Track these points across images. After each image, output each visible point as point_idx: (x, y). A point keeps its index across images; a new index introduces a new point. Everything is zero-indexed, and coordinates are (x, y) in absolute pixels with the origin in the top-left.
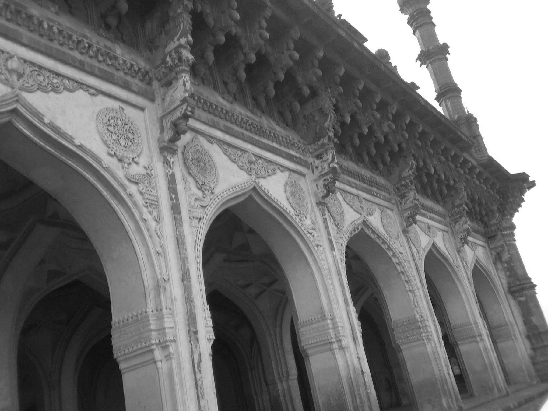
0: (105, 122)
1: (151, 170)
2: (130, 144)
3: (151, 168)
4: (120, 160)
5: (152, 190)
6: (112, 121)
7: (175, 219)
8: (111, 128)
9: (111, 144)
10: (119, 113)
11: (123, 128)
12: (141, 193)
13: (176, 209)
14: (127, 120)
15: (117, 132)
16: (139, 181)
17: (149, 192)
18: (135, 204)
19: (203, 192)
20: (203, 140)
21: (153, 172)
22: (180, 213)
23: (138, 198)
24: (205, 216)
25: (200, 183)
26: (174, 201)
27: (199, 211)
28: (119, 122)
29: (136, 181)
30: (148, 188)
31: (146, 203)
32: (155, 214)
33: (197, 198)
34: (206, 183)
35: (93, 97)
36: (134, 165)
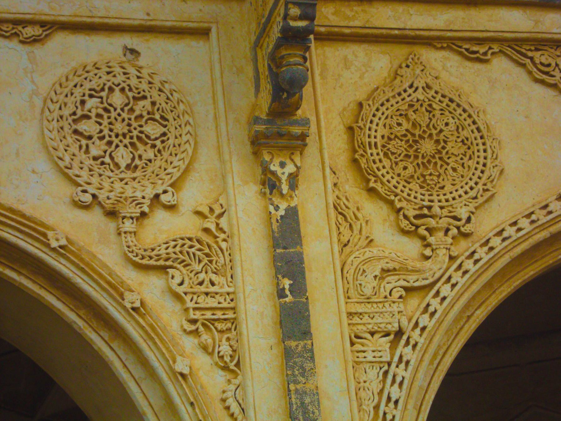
0: (66, 112)
1: (221, 215)
2: (150, 154)
3: (218, 211)
4: (112, 214)
5: (214, 277)
6: (91, 103)
7: (288, 354)
8: (84, 127)
9: (85, 174)
10: (118, 70)
11: (132, 110)
12: (177, 297)
13: (294, 322)
14: (144, 86)
15: (106, 132)
16: (169, 263)
17: (203, 289)
18: (153, 333)
19: (423, 238)
20: (446, 68)
21: (223, 222)
22: (307, 334)
23: (170, 317)
24: (424, 320)
25: (411, 213)
26: (289, 298)
27: (395, 308)
28: (117, 99)
29: (161, 263)
30: (202, 276)
31: (194, 322)
32: (225, 349)
33: (391, 266)
34: (436, 210)
35: (38, 50)
36: (160, 215)
